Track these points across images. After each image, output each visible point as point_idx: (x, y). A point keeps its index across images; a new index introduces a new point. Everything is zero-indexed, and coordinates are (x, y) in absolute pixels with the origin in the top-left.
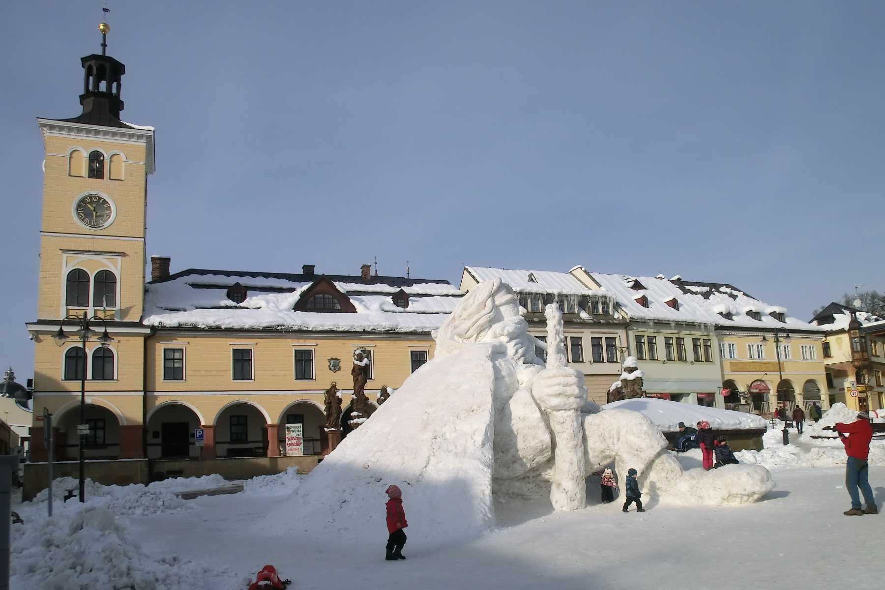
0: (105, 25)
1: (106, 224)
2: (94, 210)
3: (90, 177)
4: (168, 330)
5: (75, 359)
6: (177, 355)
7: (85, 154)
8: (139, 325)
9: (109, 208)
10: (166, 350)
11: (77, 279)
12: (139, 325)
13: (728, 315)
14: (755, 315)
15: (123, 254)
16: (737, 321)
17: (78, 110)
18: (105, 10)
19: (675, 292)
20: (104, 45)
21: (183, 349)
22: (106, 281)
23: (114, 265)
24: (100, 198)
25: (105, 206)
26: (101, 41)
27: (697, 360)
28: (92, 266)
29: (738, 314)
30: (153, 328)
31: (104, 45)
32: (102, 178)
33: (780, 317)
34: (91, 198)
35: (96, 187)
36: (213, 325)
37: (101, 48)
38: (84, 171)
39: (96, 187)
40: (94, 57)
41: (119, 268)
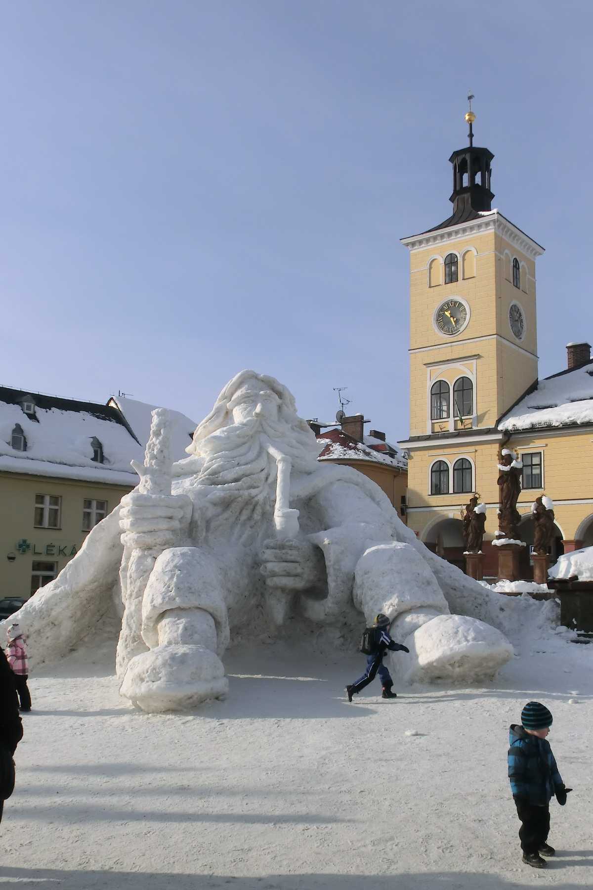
0: (471, 114)
1: (462, 329)
2: (451, 317)
4: (521, 432)
6: (536, 461)
7: (441, 261)
8: (494, 431)
10: (524, 456)
11: (439, 390)
12: (494, 431)
15: (478, 356)
18: (470, 98)
20: (471, 136)
21: (541, 453)
24: (456, 302)
26: (468, 133)
28: (451, 375)
30: (506, 433)
31: (471, 136)
34: (448, 304)
37: (468, 139)
41: (475, 372)
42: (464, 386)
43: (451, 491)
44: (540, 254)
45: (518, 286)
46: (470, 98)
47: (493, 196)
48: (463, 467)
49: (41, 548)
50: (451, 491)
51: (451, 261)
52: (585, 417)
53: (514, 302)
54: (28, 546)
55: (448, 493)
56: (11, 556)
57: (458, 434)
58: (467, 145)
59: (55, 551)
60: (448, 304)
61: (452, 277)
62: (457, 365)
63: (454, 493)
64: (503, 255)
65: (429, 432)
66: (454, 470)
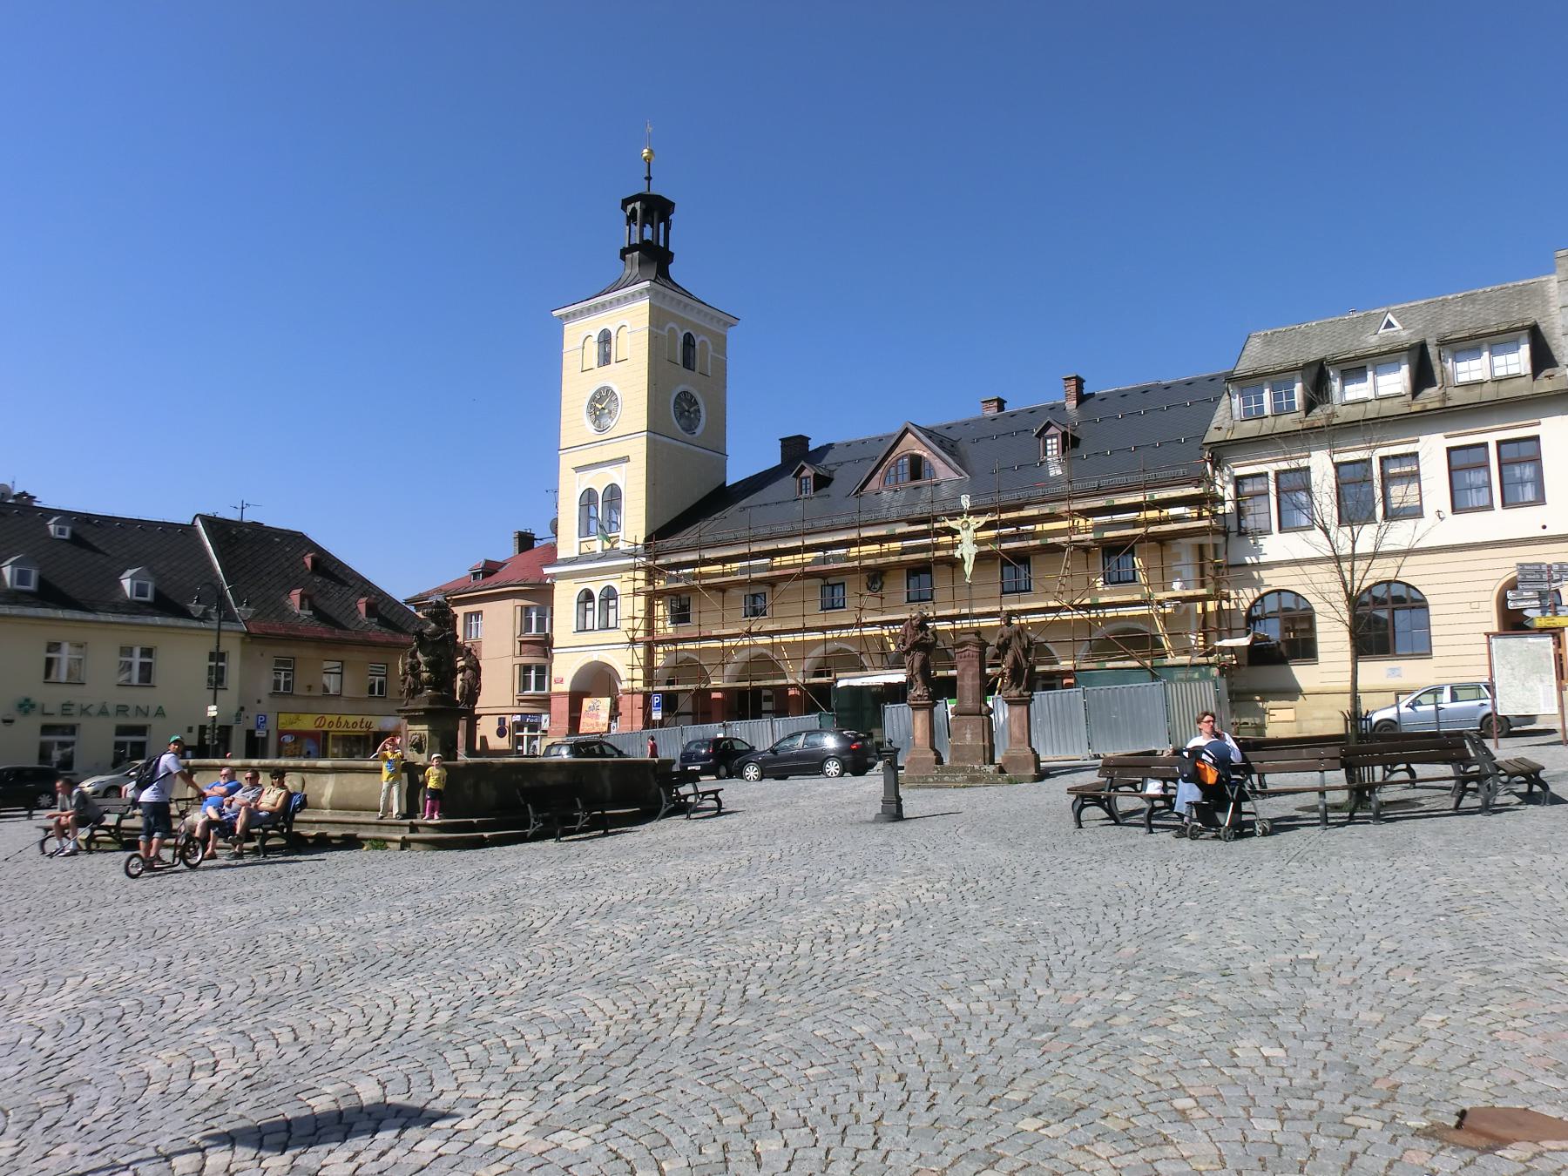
0: (651, 152)
20: (649, 178)
42: (614, 493)
44: (732, 325)
45: (692, 367)
47: (673, 254)
49: (51, 708)
51: (605, 338)
53: (681, 388)
54: (33, 706)
55: (593, 630)
56: (7, 718)
57: (605, 556)
59: (74, 710)
61: (605, 359)
63: (600, 629)
64: (663, 329)
66: (600, 600)
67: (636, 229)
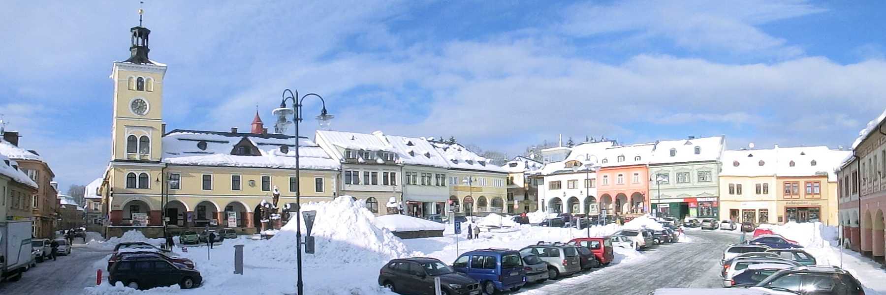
0: (141, 10)
1: (145, 113)
3: (138, 90)
5: (131, 178)
7: (135, 79)
9: (146, 105)
11: (132, 140)
13: (456, 162)
14: (470, 162)
16: (460, 166)
17: (129, 55)
18: (142, 3)
19: (429, 148)
22: (145, 140)
23: (149, 134)
24: (142, 100)
25: (144, 104)
27: (438, 185)
29: (462, 161)
30: (167, 164)
31: (141, 20)
32: (143, 90)
33: (483, 163)
35: (140, 95)
36: (194, 162)
37: (139, 22)
38: (135, 88)
39: (140, 95)
40: (137, 28)
43: (137, 187)
46: (142, 3)
48: (144, 179)
50: (137, 187)
51: (140, 80)
52: (202, 162)
58: (138, 25)
60: (138, 100)
61: (140, 87)
62: (142, 130)
65: (126, 158)
67: (135, 39)
